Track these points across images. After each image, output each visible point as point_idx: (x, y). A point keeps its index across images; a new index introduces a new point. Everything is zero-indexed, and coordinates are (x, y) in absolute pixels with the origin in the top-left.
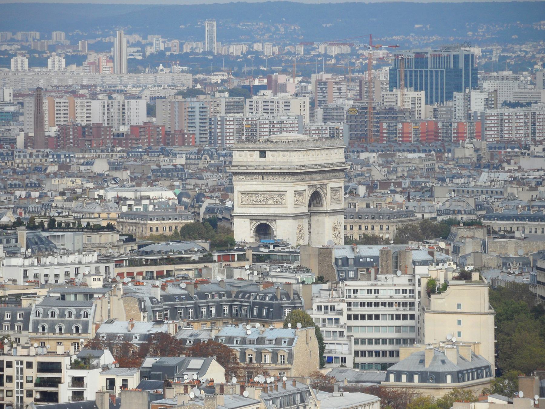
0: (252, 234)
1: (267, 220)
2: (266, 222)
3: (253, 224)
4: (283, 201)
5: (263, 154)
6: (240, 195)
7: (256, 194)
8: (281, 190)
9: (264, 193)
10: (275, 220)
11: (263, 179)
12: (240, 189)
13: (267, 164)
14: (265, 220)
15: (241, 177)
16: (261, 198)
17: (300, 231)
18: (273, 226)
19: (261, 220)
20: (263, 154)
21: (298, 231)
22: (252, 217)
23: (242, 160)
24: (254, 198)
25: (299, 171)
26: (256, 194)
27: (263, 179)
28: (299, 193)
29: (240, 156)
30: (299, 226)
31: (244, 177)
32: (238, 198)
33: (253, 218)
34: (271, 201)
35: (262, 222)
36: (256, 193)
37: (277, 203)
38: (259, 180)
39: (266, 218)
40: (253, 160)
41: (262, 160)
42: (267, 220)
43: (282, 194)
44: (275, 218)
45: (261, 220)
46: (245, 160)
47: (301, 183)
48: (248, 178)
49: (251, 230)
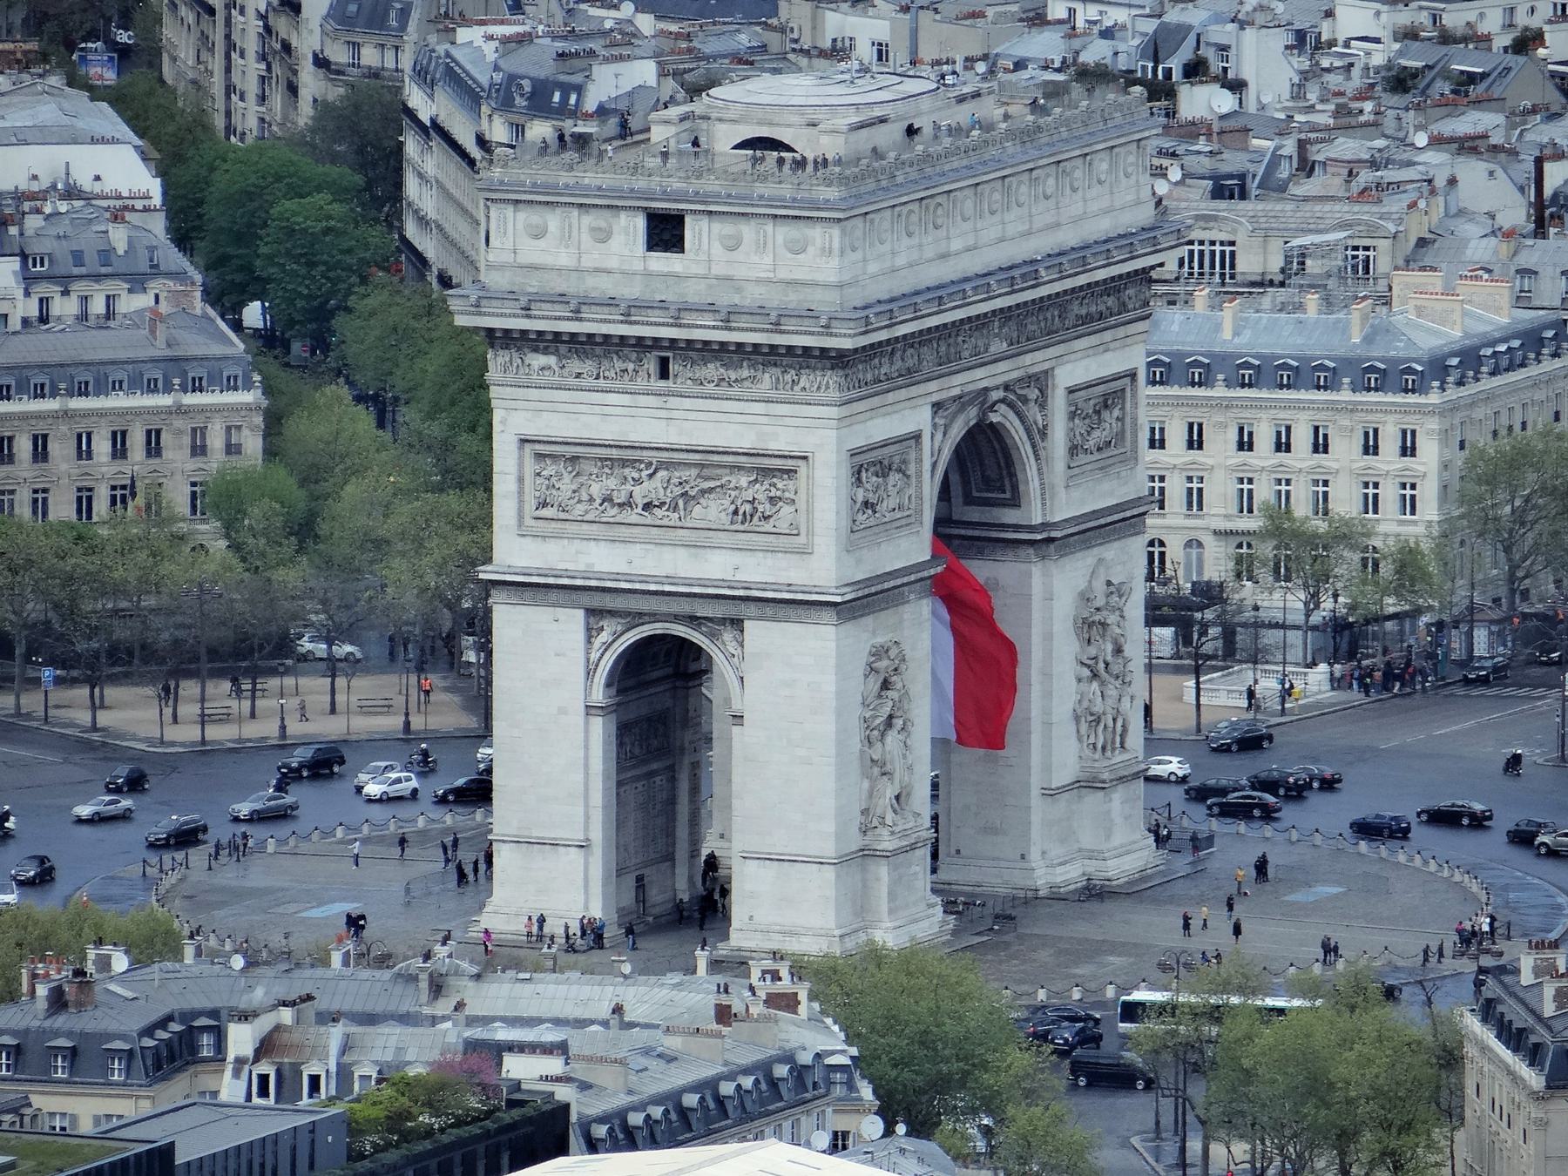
0: (599, 695)
1: (693, 620)
3: (605, 637)
4: (787, 510)
6: (530, 466)
7: (624, 463)
8: (774, 446)
9: (664, 459)
10: (737, 623)
11: (664, 374)
12: (531, 431)
13: (695, 292)
14: (676, 618)
15: (538, 360)
16: (652, 488)
17: (886, 685)
18: (719, 650)
19: (654, 617)
21: (874, 684)
23: (548, 260)
24: (612, 483)
25: (883, 336)
26: (624, 463)
27: (664, 374)
29: (539, 234)
30: (880, 652)
31: (551, 360)
32: (521, 480)
33: (609, 602)
34: (713, 511)
35: (657, 628)
37: (744, 516)
38: (641, 383)
39: (685, 607)
40: (613, 263)
41: (662, 262)
42: (693, 620)
45: (654, 617)
46: (564, 259)
47: (891, 397)
48: (575, 365)
49: (590, 673)
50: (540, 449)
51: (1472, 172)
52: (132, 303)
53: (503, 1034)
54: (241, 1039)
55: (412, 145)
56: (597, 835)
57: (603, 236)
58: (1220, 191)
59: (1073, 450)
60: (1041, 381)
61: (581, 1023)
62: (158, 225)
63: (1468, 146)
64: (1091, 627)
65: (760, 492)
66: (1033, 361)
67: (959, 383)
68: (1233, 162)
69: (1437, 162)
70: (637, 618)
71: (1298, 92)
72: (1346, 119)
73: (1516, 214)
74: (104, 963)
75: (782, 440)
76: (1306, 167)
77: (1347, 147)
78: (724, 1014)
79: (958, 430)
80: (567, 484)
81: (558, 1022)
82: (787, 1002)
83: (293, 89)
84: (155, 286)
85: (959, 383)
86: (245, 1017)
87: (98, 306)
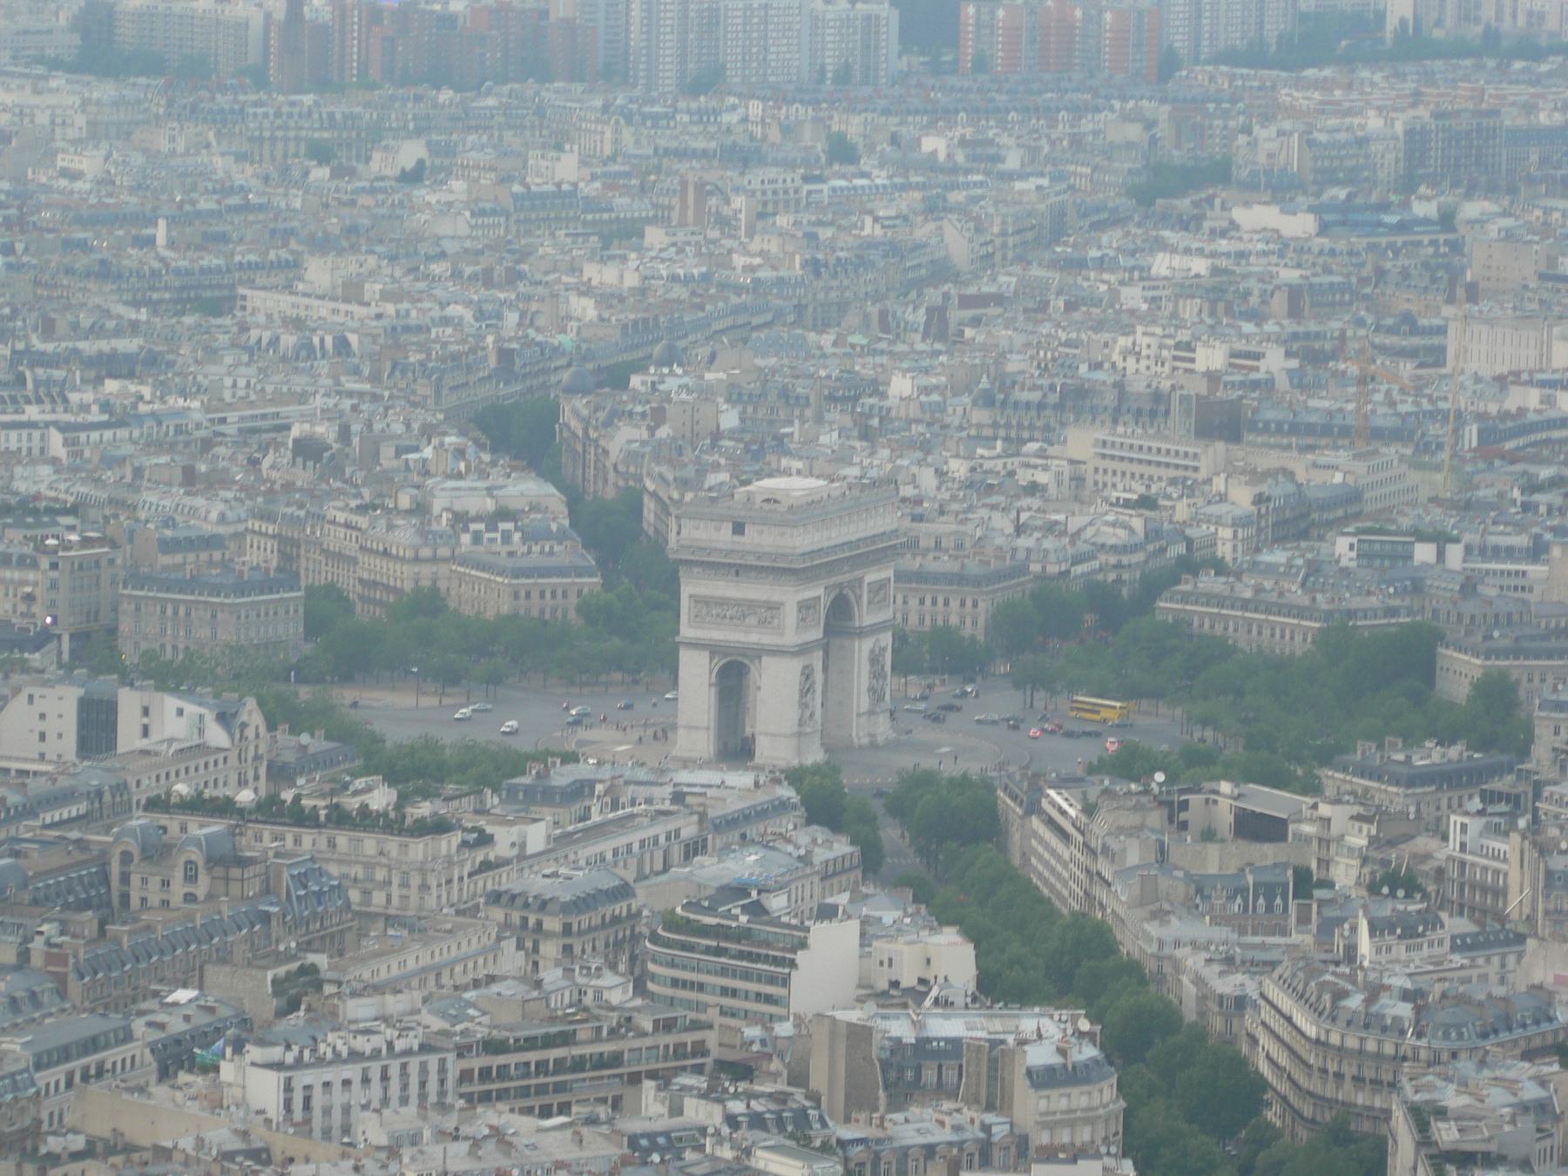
0: (713, 679)
1: (744, 655)
2: (740, 659)
5: (739, 529)
9: (738, 603)
15: (696, 570)
20: (739, 529)
22: (714, 649)
28: (805, 607)
30: (805, 667)
34: (752, 620)
36: (723, 602)
37: (763, 623)
41: (737, 538)
43: (773, 607)
44: (759, 652)
50: (696, 599)
51: (996, 515)
52: (556, 548)
53: (685, 789)
54: (599, 788)
55: (646, 499)
56: (712, 725)
57: (718, 529)
58: (913, 520)
59: (870, 602)
60: (860, 580)
61: (710, 786)
62: (566, 523)
63: (994, 507)
64: (875, 660)
65: (769, 614)
66: (858, 573)
67: (833, 580)
68: (919, 510)
69: (983, 513)
70: (725, 655)
71: (939, 488)
72: (954, 498)
73: (1010, 529)
74: (554, 764)
75: (775, 598)
76: (942, 512)
77: (955, 506)
78: (757, 784)
79: (832, 596)
80: (704, 611)
81: (703, 786)
82: (777, 781)
83: (606, 481)
84: (568, 543)
85: (833, 580)
86: (601, 781)
87: (547, 549)
